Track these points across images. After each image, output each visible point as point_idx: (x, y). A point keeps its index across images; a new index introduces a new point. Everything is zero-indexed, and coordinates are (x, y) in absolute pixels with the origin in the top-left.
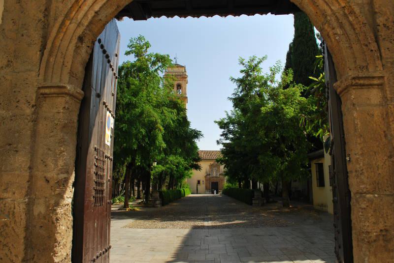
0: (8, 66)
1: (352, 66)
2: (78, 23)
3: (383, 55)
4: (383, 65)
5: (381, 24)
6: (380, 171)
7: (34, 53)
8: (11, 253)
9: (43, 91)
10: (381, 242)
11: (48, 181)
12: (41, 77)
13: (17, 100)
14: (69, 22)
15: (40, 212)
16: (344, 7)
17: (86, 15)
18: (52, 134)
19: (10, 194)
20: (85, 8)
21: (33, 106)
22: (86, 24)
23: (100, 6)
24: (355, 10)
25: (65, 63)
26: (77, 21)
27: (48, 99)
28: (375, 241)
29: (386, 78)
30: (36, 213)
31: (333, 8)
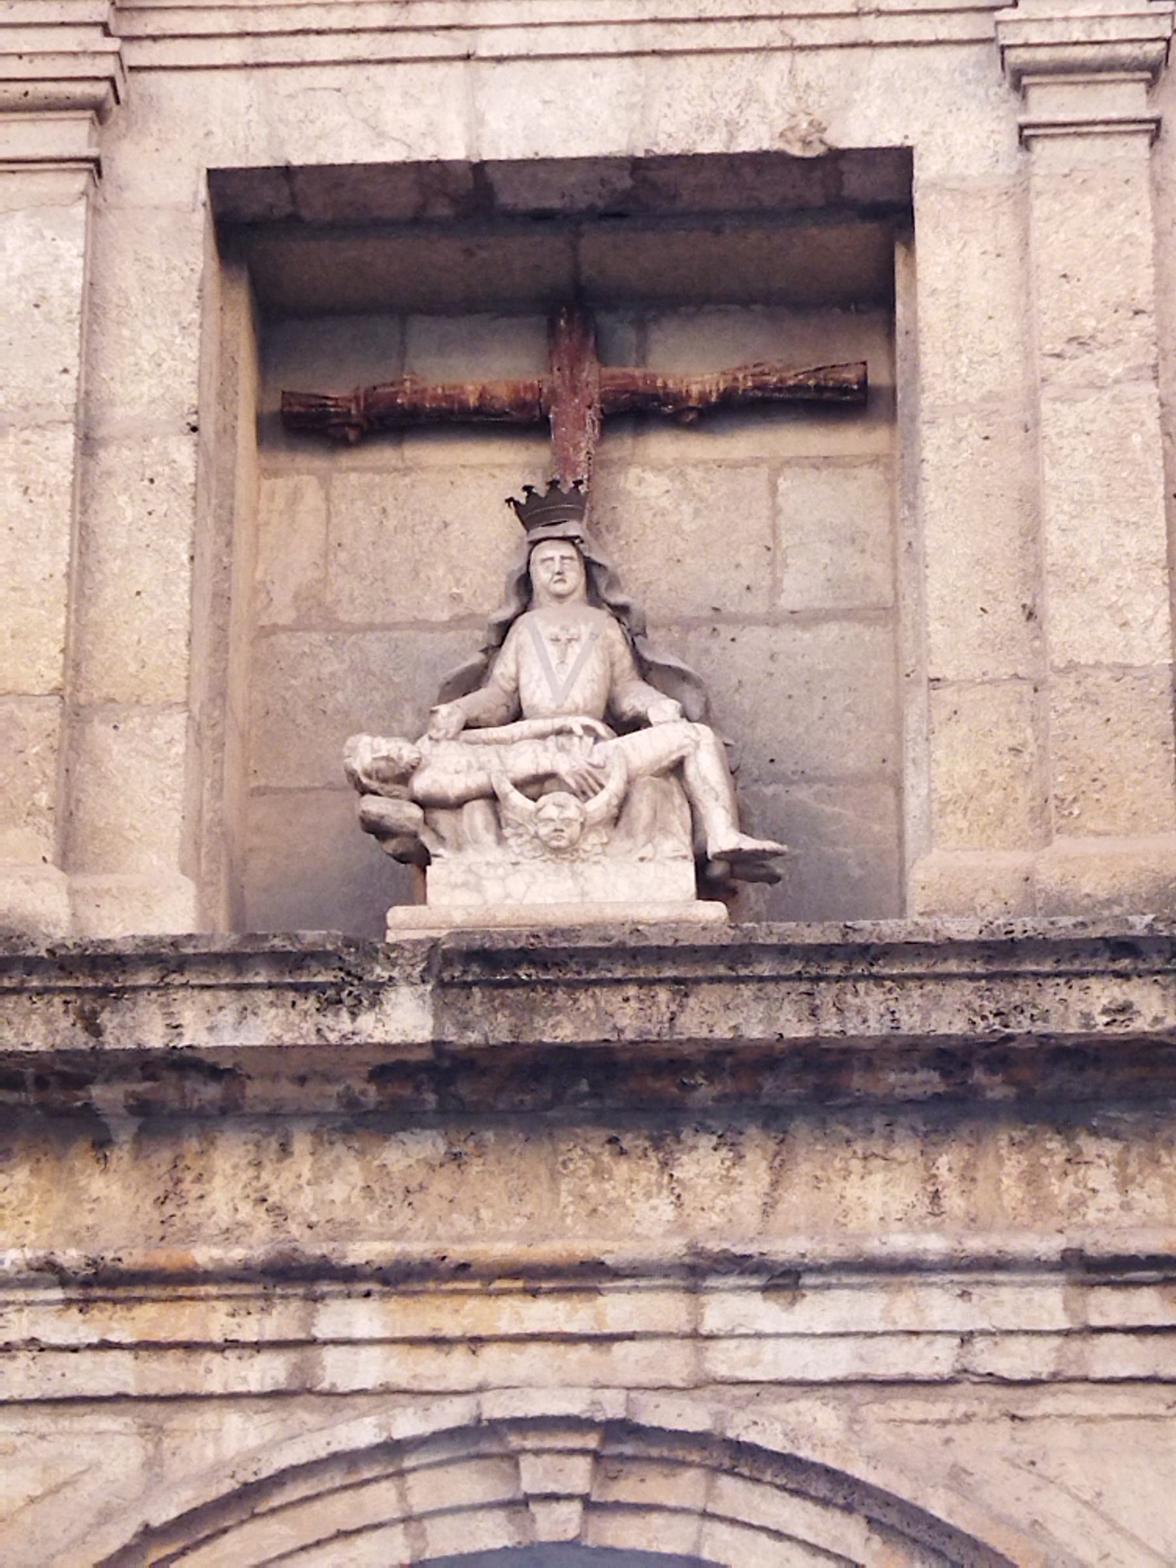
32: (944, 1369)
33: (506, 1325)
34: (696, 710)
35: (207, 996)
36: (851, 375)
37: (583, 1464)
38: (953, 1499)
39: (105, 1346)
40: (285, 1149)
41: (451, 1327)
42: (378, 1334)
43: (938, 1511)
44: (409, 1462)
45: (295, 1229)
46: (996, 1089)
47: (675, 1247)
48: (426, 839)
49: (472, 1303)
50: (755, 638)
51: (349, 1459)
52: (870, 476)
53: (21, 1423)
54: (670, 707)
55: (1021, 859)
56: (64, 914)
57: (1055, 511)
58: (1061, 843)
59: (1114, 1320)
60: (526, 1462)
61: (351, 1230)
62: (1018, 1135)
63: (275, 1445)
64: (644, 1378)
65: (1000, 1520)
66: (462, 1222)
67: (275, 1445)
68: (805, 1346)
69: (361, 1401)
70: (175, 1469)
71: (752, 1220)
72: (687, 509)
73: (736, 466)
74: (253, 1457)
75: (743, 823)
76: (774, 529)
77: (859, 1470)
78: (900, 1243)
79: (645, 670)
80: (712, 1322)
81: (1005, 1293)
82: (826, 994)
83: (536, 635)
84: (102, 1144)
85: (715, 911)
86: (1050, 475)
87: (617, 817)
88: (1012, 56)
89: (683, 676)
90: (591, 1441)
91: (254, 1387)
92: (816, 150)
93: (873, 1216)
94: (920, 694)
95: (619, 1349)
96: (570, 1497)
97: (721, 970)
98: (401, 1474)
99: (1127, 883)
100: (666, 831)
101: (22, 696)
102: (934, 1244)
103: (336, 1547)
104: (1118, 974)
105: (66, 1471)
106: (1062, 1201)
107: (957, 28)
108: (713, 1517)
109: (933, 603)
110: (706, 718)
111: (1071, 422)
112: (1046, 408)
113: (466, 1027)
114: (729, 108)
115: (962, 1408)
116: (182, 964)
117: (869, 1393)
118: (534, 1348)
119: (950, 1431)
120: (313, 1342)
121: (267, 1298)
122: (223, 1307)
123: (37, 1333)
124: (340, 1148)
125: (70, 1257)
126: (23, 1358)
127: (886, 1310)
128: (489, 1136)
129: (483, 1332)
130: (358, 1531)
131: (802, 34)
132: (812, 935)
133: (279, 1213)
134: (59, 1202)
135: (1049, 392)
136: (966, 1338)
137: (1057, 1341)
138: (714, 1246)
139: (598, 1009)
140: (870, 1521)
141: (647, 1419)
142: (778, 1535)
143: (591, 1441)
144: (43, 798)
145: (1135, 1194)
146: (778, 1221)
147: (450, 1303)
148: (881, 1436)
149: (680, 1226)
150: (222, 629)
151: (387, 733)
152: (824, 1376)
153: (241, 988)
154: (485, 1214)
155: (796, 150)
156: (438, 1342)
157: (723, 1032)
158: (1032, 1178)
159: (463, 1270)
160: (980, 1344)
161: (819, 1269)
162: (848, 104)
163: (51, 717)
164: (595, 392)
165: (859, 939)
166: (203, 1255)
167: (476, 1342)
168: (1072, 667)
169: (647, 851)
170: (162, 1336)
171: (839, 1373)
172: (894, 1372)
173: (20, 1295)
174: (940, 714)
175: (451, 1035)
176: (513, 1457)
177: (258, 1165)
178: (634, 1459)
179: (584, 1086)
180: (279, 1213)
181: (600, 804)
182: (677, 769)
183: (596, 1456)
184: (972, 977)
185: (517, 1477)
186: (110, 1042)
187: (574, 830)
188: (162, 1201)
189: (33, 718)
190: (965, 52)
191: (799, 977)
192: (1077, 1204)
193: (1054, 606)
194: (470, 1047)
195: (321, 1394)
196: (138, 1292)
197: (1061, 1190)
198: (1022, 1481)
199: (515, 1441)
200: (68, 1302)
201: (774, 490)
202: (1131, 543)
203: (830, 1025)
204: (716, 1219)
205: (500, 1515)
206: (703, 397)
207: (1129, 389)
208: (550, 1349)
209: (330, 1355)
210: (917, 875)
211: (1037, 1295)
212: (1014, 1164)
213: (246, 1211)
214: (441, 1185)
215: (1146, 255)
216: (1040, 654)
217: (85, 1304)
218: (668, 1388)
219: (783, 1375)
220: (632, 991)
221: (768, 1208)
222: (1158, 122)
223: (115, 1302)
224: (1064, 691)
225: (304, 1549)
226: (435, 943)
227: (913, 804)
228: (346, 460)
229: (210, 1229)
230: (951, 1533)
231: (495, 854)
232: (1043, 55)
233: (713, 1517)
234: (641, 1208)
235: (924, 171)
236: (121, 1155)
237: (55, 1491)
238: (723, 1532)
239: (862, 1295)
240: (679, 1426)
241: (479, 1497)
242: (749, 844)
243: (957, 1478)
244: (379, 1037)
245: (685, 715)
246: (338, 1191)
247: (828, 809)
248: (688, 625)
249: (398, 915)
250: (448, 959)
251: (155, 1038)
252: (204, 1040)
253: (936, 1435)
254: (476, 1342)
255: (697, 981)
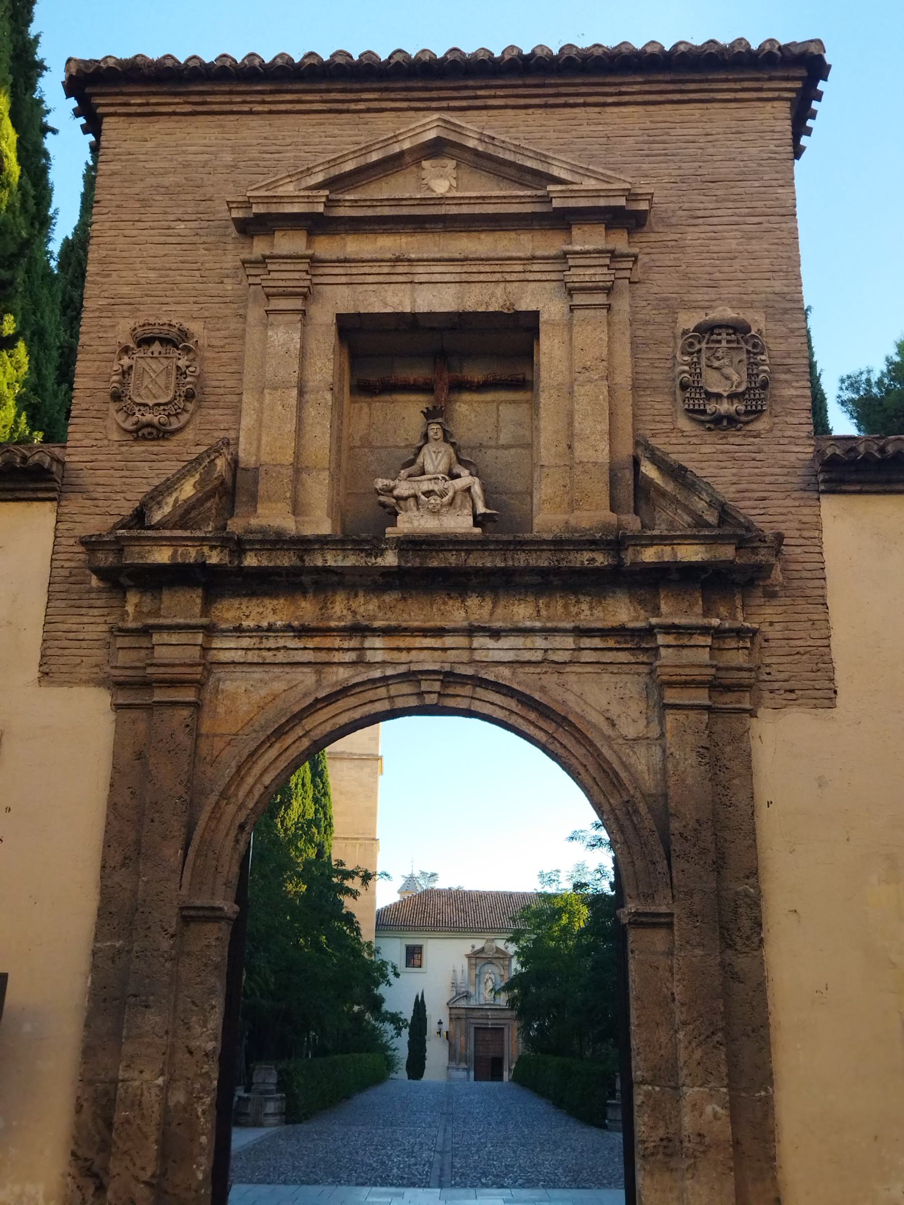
0: (123, 865)
1: (634, 894)
2: (239, 804)
3: (675, 880)
4: (673, 897)
5: (676, 832)
6: (662, 1052)
7: (172, 852)
8: (134, 1164)
9: (185, 913)
10: (660, 1157)
11: (191, 1053)
12: (184, 892)
13: (148, 926)
14: (225, 802)
15: (179, 1102)
16: (628, 802)
17: (250, 791)
18: (199, 979)
19: (136, 1074)
20: (250, 780)
21: (172, 936)
22: (251, 805)
23: (273, 777)
24: (641, 809)
25: (220, 869)
26: (237, 801)
27: (192, 925)
28: (652, 1154)
29: (676, 916)
30: (171, 1104)
31: (612, 801)
32: (540, 659)
33: (417, 645)
34: (474, 473)
35: (334, 552)
36: (520, 377)
37: (438, 683)
38: (542, 695)
39: (305, 648)
40: (356, 595)
41: (402, 645)
42: (382, 646)
43: (537, 698)
44: (390, 682)
45: (359, 617)
46: (556, 581)
47: (465, 624)
48: (397, 508)
49: (408, 639)
50: (491, 452)
51: (373, 681)
52: (525, 406)
53: (282, 669)
54: (467, 472)
55: (566, 517)
56: (294, 528)
57: (577, 417)
58: (577, 512)
59: (588, 646)
60: (423, 683)
61: (375, 618)
62: (562, 595)
63: (353, 677)
64: (456, 660)
65: (554, 700)
66: (405, 616)
67: (353, 677)
68: (501, 652)
69: (377, 665)
70: (325, 683)
71: (486, 616)
72: (473, 415)
73: (487, 402)
74: (346, 680)
75: (487, 505)
76: (498, 421)
77: (515, 686)
78: (528, 624)
79: (460, 461)
80: (475, 644)
81: (557, 638)
82: (509, 554)
83: (429, 451)
84: (304, 593)
85: (478, 530)
86: (576, 407)
87: (451, 503)
88: (568, 285)
89: (471, 463)
90: (441, 677)
91: (347, 660)
92: (512, 311)
93: (521, 617)
94: (538, 469)
95: (449, 652)
96: (435, 692)
97: (479, 547)
98: (388, 685)
99: (595, 524)
100: (465, 508)
101: (282, 465)
102: (538, 624)
103: (369, 705)
104: (591, 550)
105: (294, 683)
106: (574, 613)
107: (553, 276)
108: (474, 698)
109: (542, 443)
110: (477, 476)
111: (583, 392)
112: (576, 388)
113: (407, 562)
114: (487, 299)
115: (544, 670)
116: (327, 543)
117: (518, 665)
118: (425, 652)
119: (541, 676)
120: (364, 649)
121: (351, 636)
122: (338, 639)
123: (286, 644)
124: (372, 595)
125: (296, 623)
126: (282, 651)
127: (524, 643)
128: (414, 592)
129: (411, 646)
130: (376, 701)
131: (508, 277)
132: (505, 538)
133: (354, 613)
134: (292, 608)
135: (577, 383)
136: (546, 650)
137: (571, 652)
138: (476, 624)
139: (445, 558)
140: (518, 700)
141: (457, 671)
142: (492, 704)
143: (441, 677)
144: (288, 495)
145: (595, 611)
146: (495, 616)
147: (402, 639)
148: (522, 677)
149: (467, 619)
150: (340, 447)
151: (386, 478)
152: (506, 660)
153: (344, 550)
154: (412, 614)
155: (506, 311)
156: (399, 649)
157: (480, 565)
158: (566, 606)
159: (406, 629)
160: (550, 652)
161: (504, 631)
162: (521, 298)
163: (290, 472)
164: (447, 380)
165: (518, 539)
166: (333, 624)
167: (409, 650)
168: (581, 462)
169: (460, 513)
170: (321, 646)
171: (510, 659)
172: (526, 659)
173: (281, 634)
174: (544, 475)
175: (403, 564)
176: (419, 681)
177: (349, 599)
178: (452, 682)
179: (440, 579)
180: (354, 613)
181: (446, 499)
182: (468, 490)
183: (442, 681)
184: (550, 550)
185: (420, 686)
186: (307, 564)
187: (439, 506)
188: (321, 609)
189: (285, 472)
190: (555, 283)
191: (501, 549)
192: (578, 614)
193: (577, 445)
194: (409, 568)
195: (367, 663)
196: (315, 634)
197: (574, 610)
198: (560, 690)
199: (420, 677)
200: (295, 637)
201: (498, 409)
202: (599, 427)
203: (510, 563)
204: (477, 617)
205: (415, 697)
206: (478, 382)
207: (600, 383)
208: (430, 652)
209: (368, 653)
210: (536, 521)
211: (566, 639)
212: (561, 603)
213: (345, 612)
214: (400, 606)
215: (605, 344)
216: (572, 458)
217: (300, 637)
218: (463, 663)
219: (495, 660)
220: (454, 553)
221: (491, 614)
222: (610, 305)
223: (308, 636)
224: (578, 470)
225: (361, 705)
226: (399, 538)
227: (535, 500)
228: (376, 399)
229: (335, 616)
230: (540, 704)
231: (416, 513)
232: (577, 285)
233: (474, 698)
234: (456, 613)
235: (543, 318)
236: (310, 596)
237: (291, 688)
238: (477, 703)
239: (517, 638)
240: (465, 673)
241: (409, 692)
242: (488, 511)
243: (543, 689)
244: (383, 564)
245: (471, 474)
246: (371, 607)
247: (512, 502)
248: (473, 448)
249: (388, 530)
250: (403, 542)
251: (320, 563)
252: (333, 564)
253: (536, 677)
254: (409, 650)
255: (473, 550)
